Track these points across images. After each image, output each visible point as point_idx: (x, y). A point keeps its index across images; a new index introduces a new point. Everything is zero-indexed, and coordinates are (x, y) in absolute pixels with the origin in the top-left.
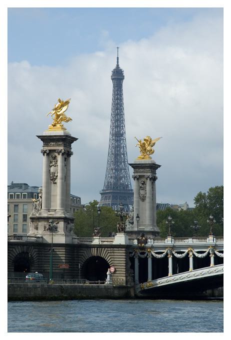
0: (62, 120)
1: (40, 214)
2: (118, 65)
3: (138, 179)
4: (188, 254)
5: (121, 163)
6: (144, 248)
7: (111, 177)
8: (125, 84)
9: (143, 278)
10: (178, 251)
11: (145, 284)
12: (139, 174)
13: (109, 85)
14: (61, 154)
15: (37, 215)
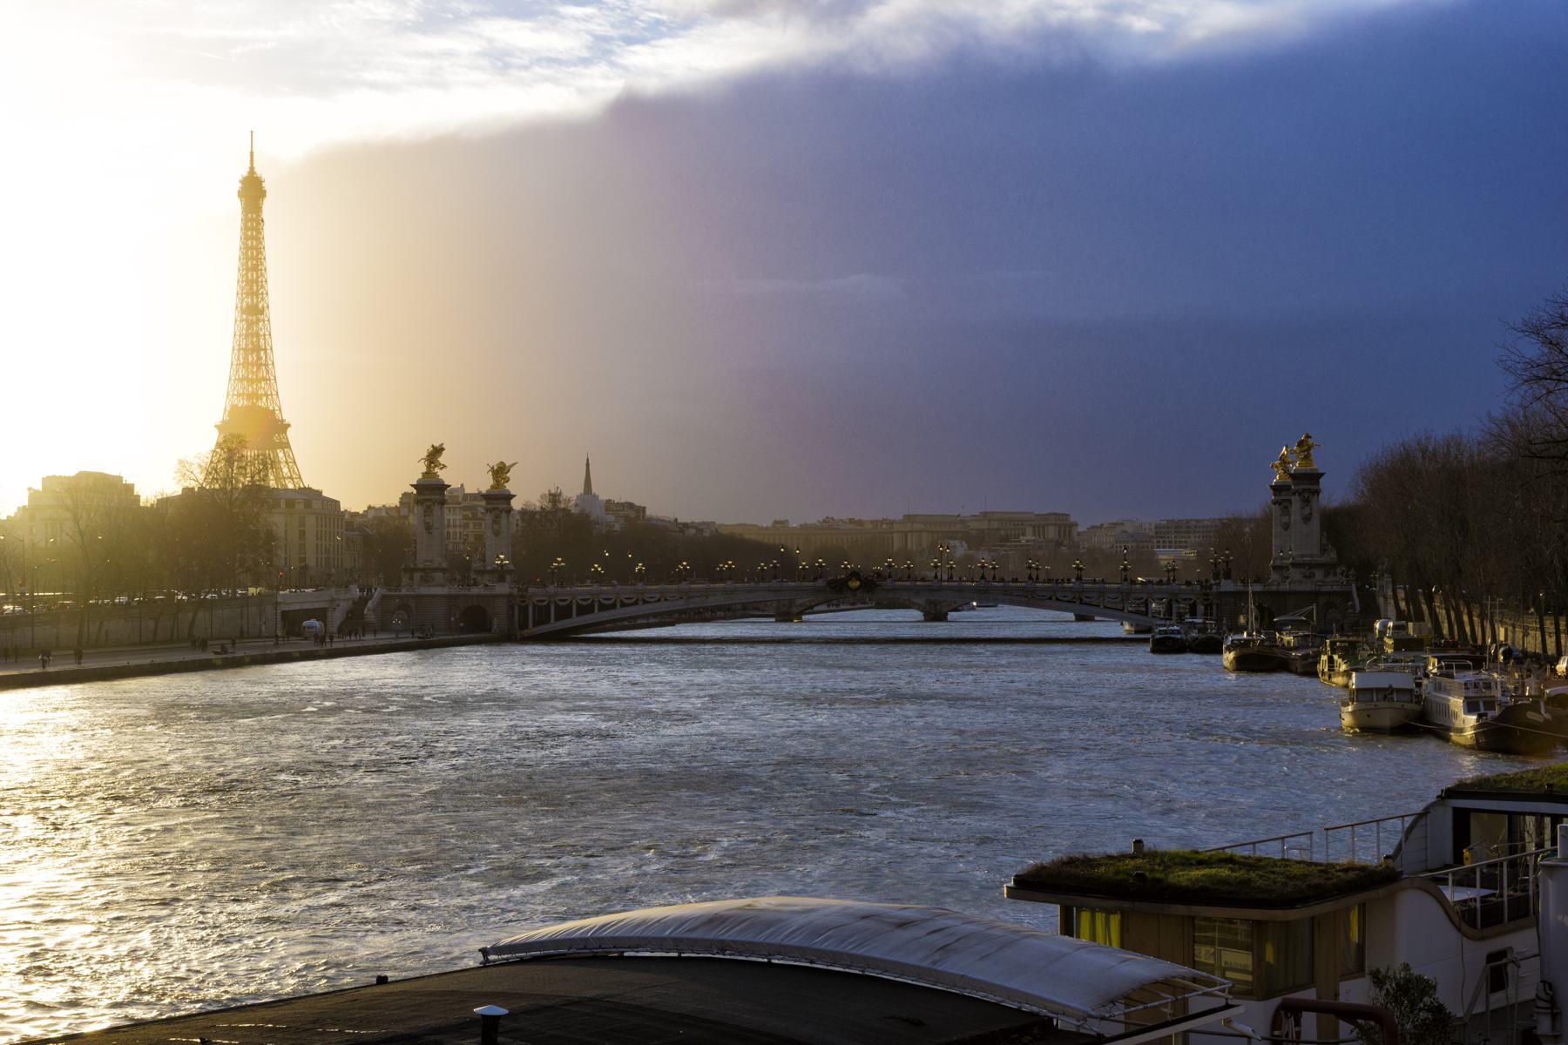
0: (436, 466)
1: (415, 564)
2: (252, 168)
3: (491, 512)
4: (571, 602)
5: (258, 369)
6: (523, 597)
7: (239, 395)
8: (268, 206)
9: (524, 626)
10: (560, 598)
11: (525, 631)
12: (491, 506)
13: (235, 206)
14: (436, 504)
15: (412, 566)
